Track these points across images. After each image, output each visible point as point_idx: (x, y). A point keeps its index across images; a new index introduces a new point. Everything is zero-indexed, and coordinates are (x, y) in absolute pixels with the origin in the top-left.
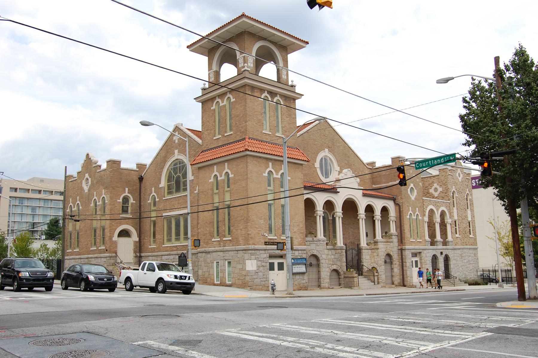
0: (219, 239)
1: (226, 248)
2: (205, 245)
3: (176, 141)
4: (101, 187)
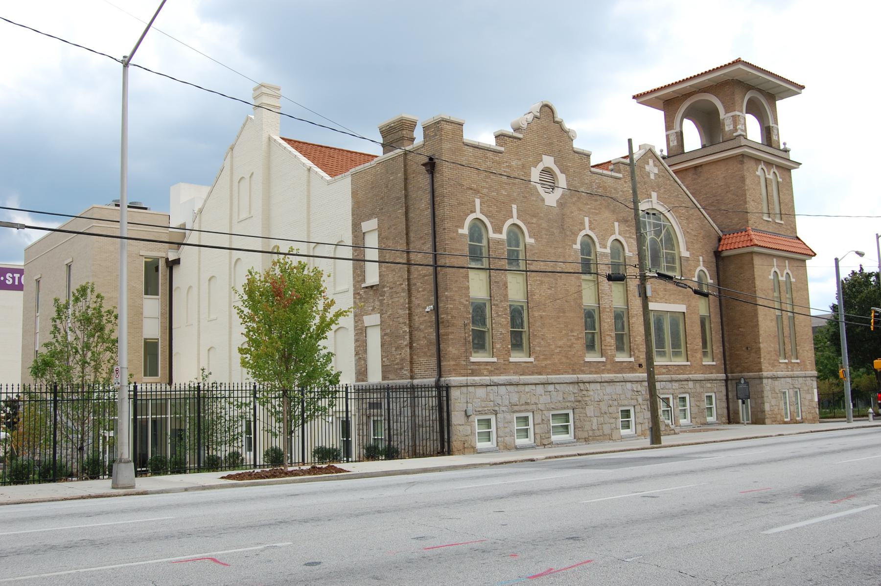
0: (786, 361)
1: (796, 373)
2: (770, 368)
3: (652, 177)
4: (606, 214)
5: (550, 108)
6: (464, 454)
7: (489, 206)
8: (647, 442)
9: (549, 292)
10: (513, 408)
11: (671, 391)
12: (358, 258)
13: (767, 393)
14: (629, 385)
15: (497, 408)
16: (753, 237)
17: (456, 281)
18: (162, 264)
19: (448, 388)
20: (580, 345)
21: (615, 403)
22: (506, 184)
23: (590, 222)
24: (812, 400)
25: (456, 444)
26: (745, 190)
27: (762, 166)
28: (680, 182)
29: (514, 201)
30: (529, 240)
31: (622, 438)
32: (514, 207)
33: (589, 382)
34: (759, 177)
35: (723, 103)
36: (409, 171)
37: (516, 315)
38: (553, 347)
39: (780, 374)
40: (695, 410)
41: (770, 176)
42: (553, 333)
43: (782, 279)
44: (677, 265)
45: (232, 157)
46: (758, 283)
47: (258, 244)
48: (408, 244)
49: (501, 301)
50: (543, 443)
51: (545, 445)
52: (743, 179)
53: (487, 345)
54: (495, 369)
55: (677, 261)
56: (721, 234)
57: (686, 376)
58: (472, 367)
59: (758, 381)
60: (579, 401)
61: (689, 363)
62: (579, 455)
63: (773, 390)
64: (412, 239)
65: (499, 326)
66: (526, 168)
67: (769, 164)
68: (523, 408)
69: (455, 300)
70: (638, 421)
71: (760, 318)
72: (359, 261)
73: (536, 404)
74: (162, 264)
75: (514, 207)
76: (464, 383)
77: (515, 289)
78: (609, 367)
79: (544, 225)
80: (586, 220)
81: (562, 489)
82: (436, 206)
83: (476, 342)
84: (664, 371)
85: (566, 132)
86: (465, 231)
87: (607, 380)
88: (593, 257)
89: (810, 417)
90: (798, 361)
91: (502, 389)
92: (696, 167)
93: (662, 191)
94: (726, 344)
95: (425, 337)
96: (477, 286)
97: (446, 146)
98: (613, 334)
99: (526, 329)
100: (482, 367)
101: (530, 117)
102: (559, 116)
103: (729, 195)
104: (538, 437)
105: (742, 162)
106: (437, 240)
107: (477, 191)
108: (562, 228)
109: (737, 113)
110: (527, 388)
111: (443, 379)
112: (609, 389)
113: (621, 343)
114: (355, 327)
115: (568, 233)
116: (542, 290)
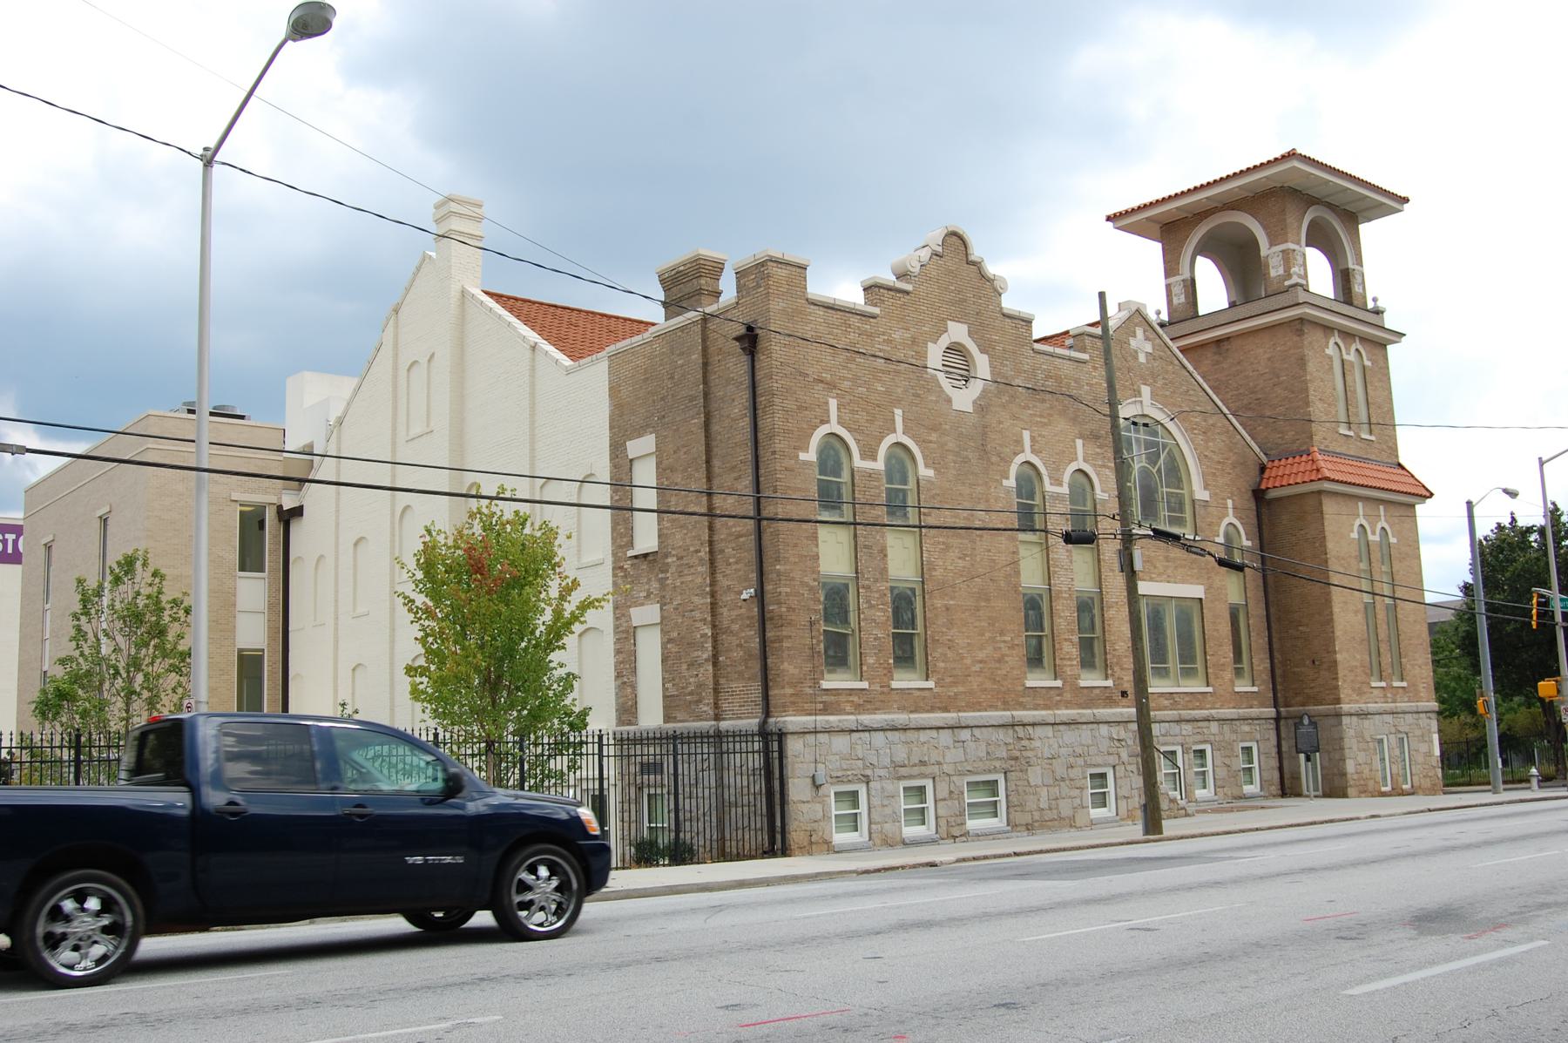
0: (1383, 684)
2: (1355, 697)
3: (1142, 358)
4: (1061, 425)
5: (960, 238)
6: (810, 854)
7: (853, 412)
8: (1136, 830)
9: (961, 563)
10: (897, 770)
11: (1179, 739)
12: (620, 504)
13: (1350, 742)
14: (1104, 729)
15: (868, 772)
16: (1322, 464)
17: (796, 545)
18: (270, 517)
19: (781, 736)
20: (1016, 658)
21: (1080, 761)
22: (883, 372)
23: (1033, 439)
24: (1429, 754)
25: (796, 836)
26: (1305, 382)
27: (1336, 338)
28: (1190, 368)
29: (897, 402)
30: (925, 472)
31: (1093, 824)
32: (898, 412)
33: (1033, 725)
34: (1330, 358)
35: (1265, 228)
36: (712, 349)
37: (902, 605)
38: (968, 661)
39: (1372, 707)
40: (1222, 773)
41: (1351, 357)
42: (971, 637)
43: (1374, 538)
44: (1188, 515)
45: (396, 326)
46: (1330, 545)
47: (442, 481)
48: (709, 479)
49: (876, 581)
50: (952, 833)
51: (955, 837)
52: (1302, 362)
53: (851, 658)
54: (865, 702)
55: (1188, 508)
56: (1264, 459)
57: (1204, 713)
58: (825, 698)
59: (1332, 721)
60: (1016, 759)
61: (1210, 689)
62: (1016, 854)
63: (1360, 736)
64: (716, 470)
65: (872, 625)
66: (918, 344)
67: (1347, 335)
68: (916, 770)
69: (793, 579)
70: (1121, 793)
71: (1336, 609)
72: (622, 510)
73: (939, 763)
74: (270, 517)
75: (898, 412)
76: (811, 727)
77: (901, 558)
78: (1068, 696)
79: (951, 446)
80: (1026, 435)
81: (985, 917)
82: (759, 412)
83: (831, 653)
84: (1166, 703)
85: (989, 280)
86: (810, 455)
87: (1065, 719)
88: (1038, 501)
89: (1427, 783)
90: (1404, 684)
91: (879, 738)
92: (1219, 342)
93: (1160, 383)
94: (1277, 655)
95: (740, 645)
96: (833, 554)
97: (777, 305)
98: (1075, 638)
99: (920, 629)
100: (843, 698)
101: (925, 254)
102: (976, 252)
103: (1279, 390)
104: (943, 822)
105: (1300, 333)
106: (762, 471)
107: (831, 386)
108: (983, 451)
109: (1291, 246)
110: (924, 736)
111: (772, 720)
112: (1069, 735)
113: (1091, 652)
114: (616, 627)
115: (994, 459)
116: (949, 559)
